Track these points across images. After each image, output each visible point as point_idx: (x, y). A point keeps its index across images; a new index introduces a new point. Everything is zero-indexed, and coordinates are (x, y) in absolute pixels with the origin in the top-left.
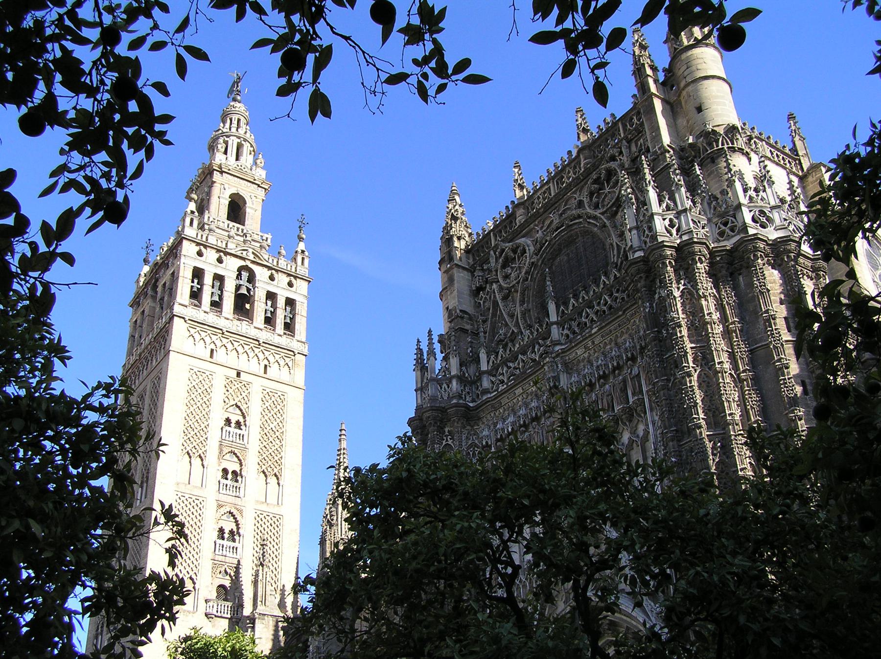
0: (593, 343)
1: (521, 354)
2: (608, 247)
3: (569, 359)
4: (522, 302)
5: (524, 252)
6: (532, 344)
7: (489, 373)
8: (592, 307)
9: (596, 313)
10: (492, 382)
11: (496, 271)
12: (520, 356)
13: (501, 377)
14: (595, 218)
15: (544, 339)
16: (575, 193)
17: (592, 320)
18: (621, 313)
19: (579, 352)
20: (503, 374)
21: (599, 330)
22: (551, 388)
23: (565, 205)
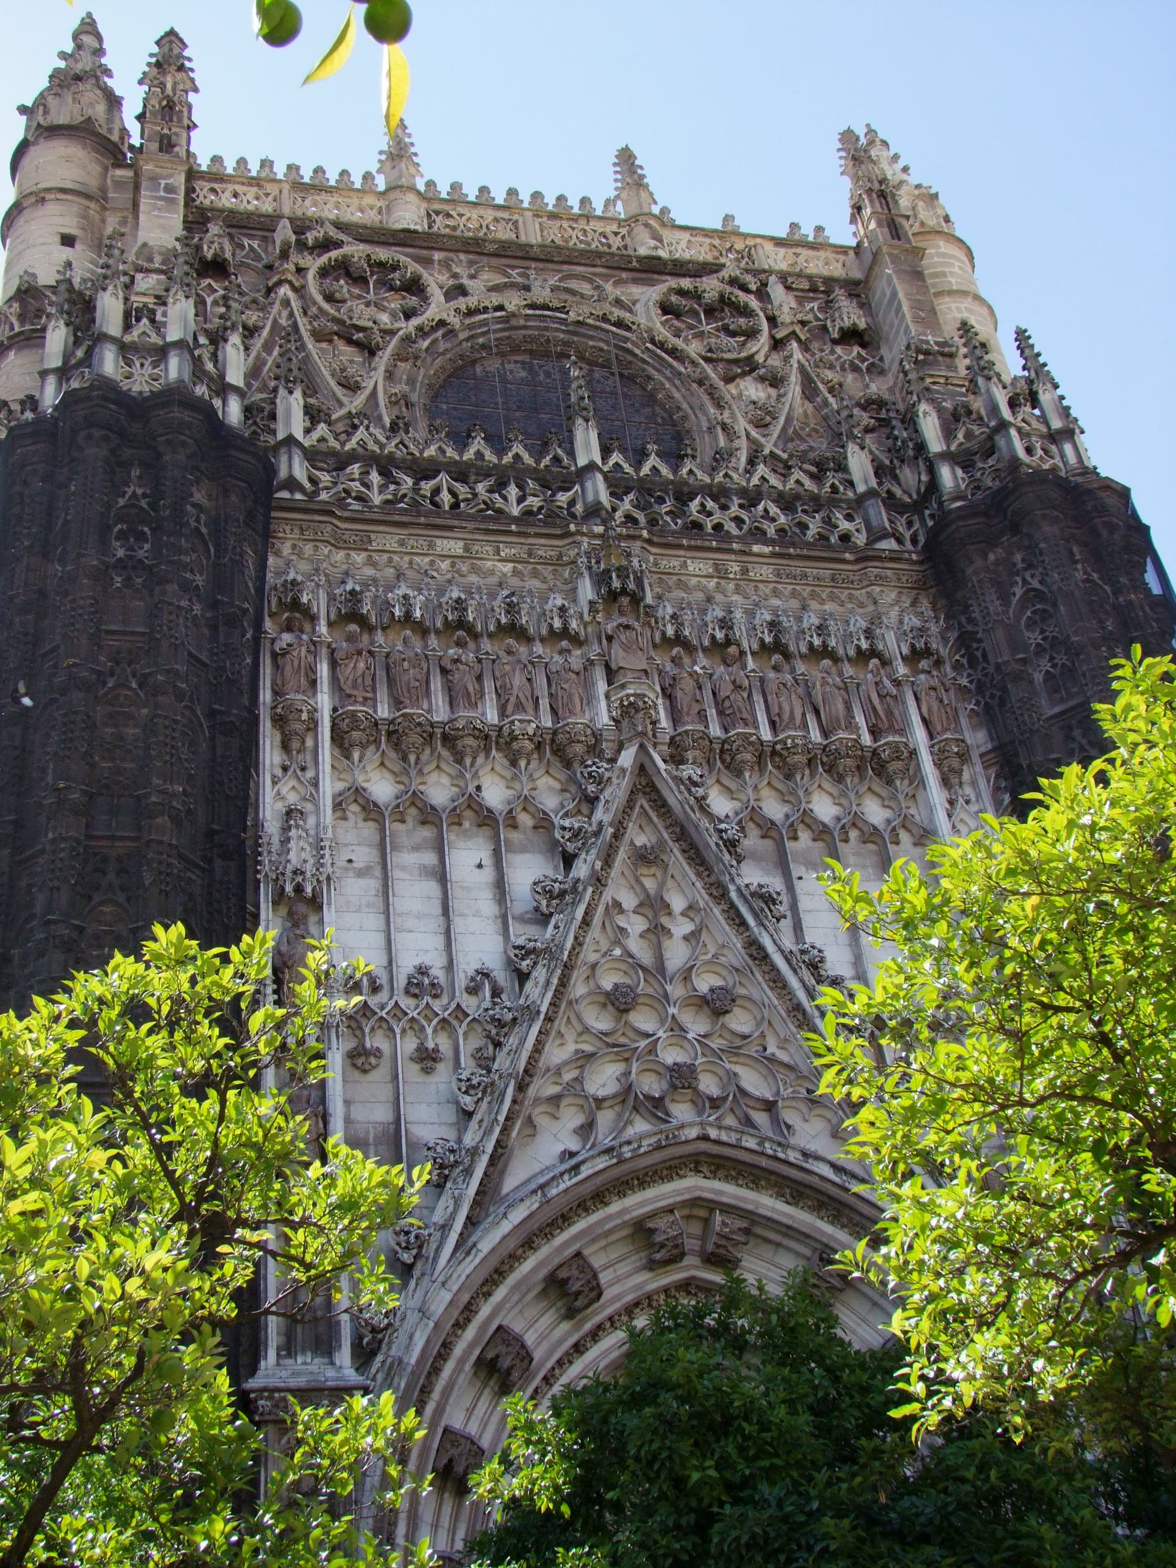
0: (745, 571)
1: (449, 473)
2: (705, 425)
3: (656, 564)
4: (390, 376)
5: (414, 287)
6: (517, 474)
7: (312, 456)
8: (724, 508)
9: (738, 521)
10: (313, 481)
11: (300, 270)
12: (443, 478)
13: (356, 486)
14: (673, 352)
15: (545, 485)
16: (606, 278)
17: (718, 527)
18: (847, 556)
19: (692, 567)
20: (367, 486)
21: (774, 555)
22: (624, 592)
23: (560, 280)
